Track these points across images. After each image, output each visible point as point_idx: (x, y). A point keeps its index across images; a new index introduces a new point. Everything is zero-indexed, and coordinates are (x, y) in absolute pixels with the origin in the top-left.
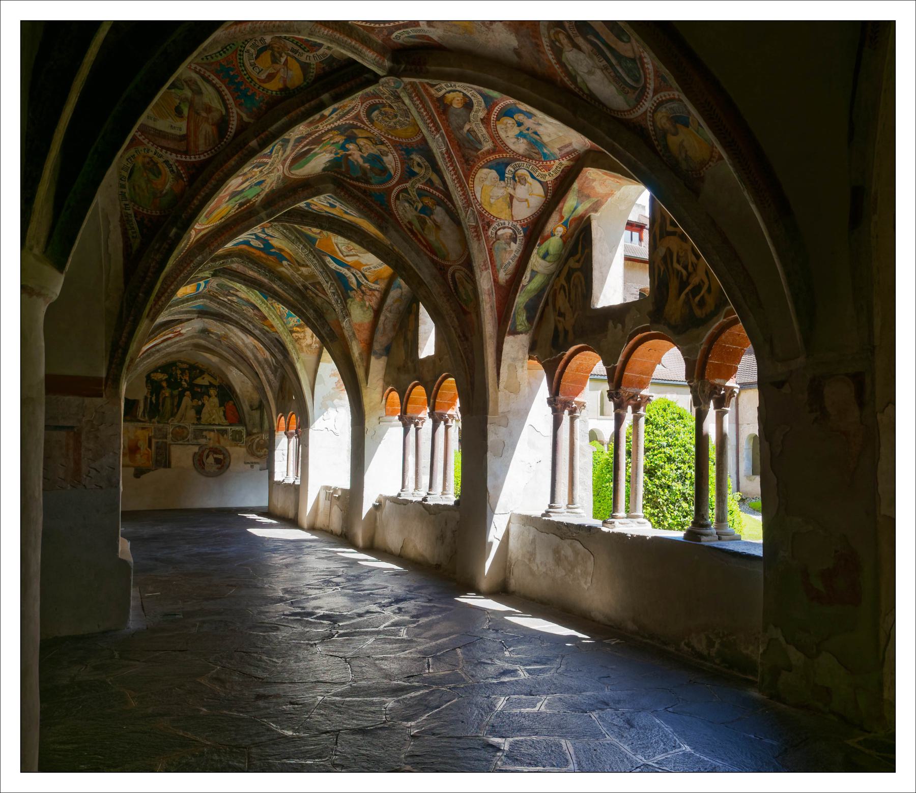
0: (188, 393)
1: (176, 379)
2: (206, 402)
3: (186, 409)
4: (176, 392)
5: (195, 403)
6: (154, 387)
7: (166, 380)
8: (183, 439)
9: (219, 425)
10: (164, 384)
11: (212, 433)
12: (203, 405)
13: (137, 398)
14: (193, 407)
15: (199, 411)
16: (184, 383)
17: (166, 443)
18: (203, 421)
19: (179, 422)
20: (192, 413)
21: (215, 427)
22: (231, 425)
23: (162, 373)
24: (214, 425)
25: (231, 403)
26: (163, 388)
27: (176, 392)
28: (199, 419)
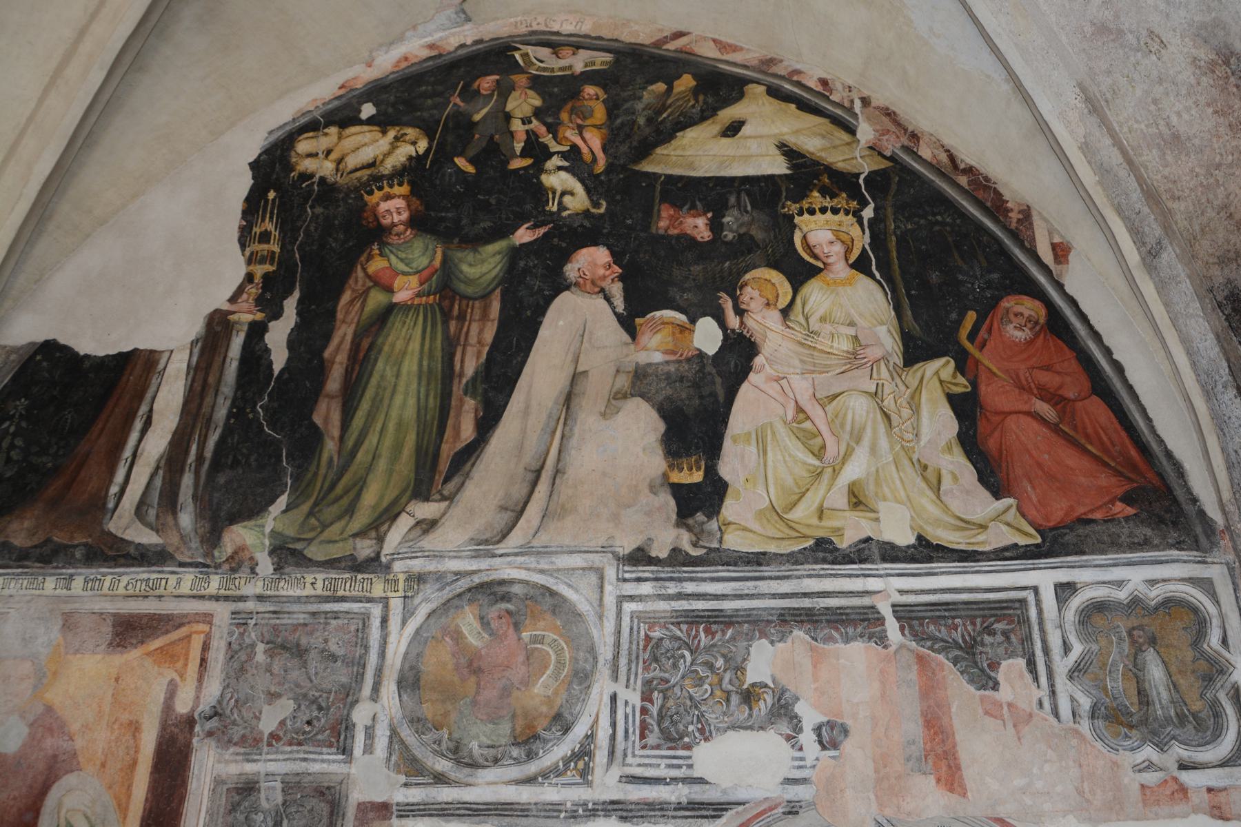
0: (592, 260)
1: (492, 154)
2: (763, 323)
3: (569, 399)
4: (483, 265)
5: (653, 348)
6: (302, 225)
7: (413, 171)
8: (528, 741)
9: (926, 551)
10: (393, 207)
11: (854, 654)
12: (740, 352)
13: (143, 342)
14: (640, 382)
15: (695, 419)
16: (557, 179)
17: (330, 796)
18: (743, 521)
19: (487, 544)
20: (627, 443)
21: (888, 587)
22: (1054, 542)
23: (381, 122)
24: (869, 552)
25: (1018, 319)
26: (378, 234)
27: (483, 265)
28: (700, 500)
